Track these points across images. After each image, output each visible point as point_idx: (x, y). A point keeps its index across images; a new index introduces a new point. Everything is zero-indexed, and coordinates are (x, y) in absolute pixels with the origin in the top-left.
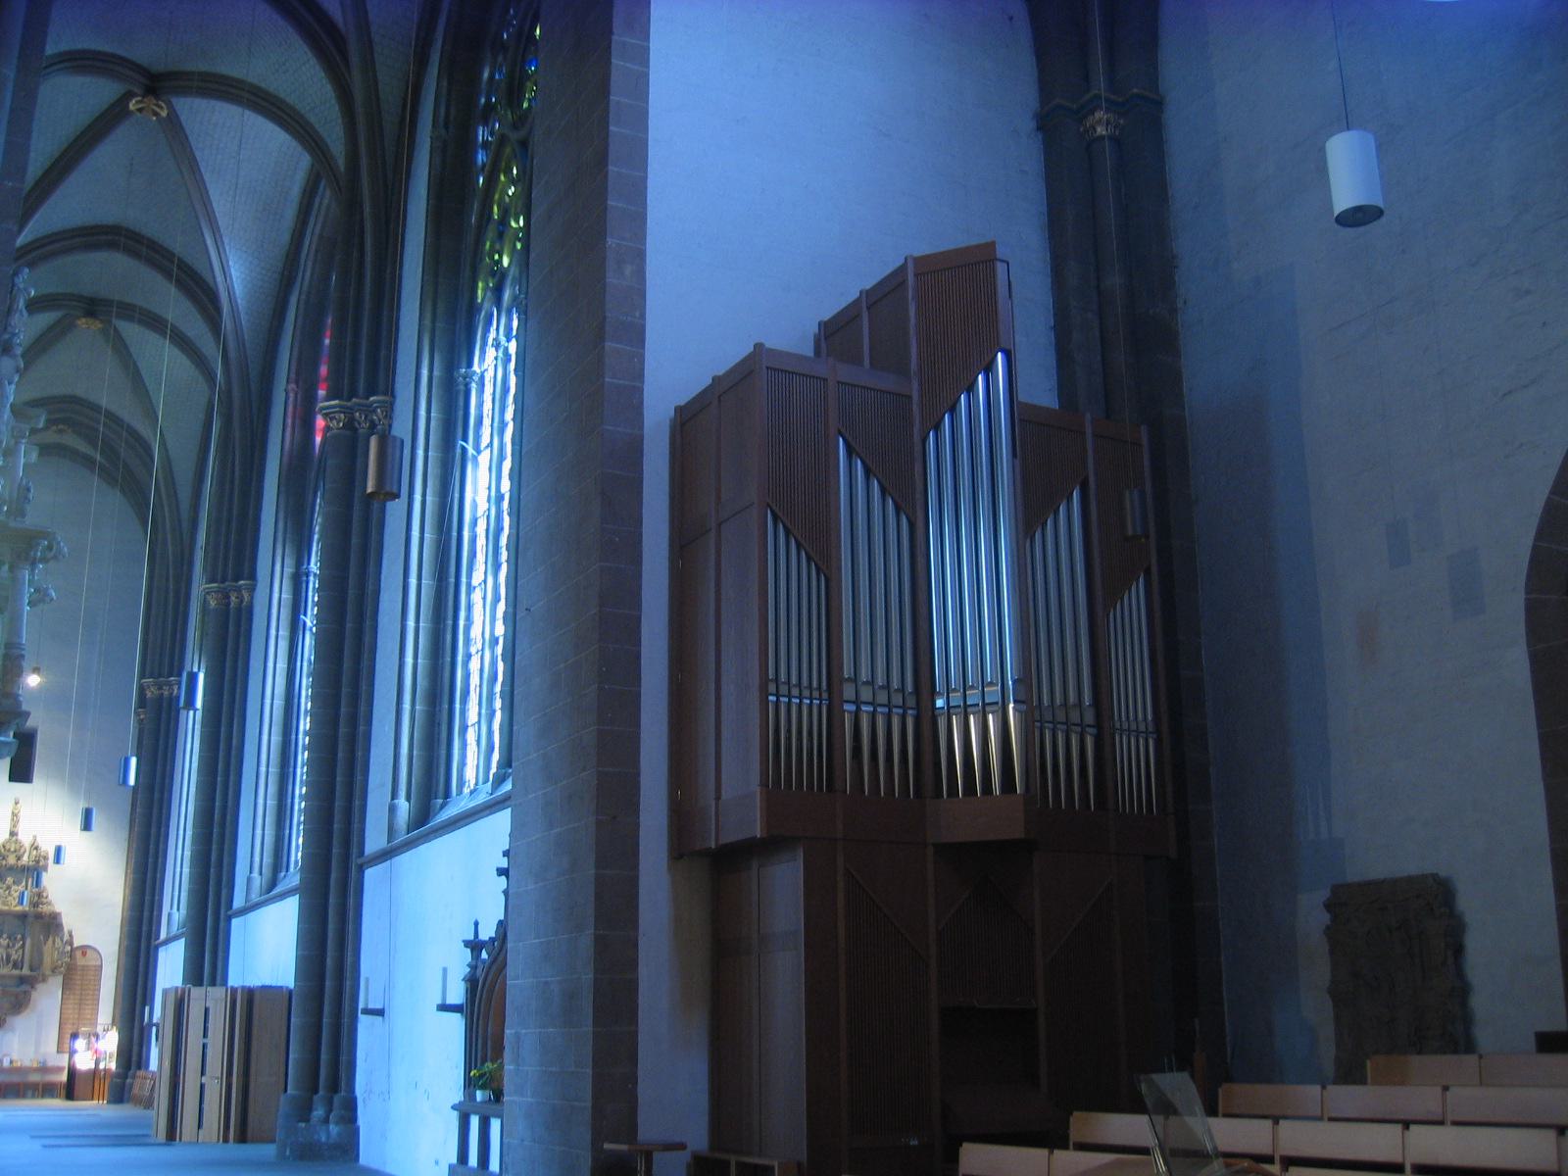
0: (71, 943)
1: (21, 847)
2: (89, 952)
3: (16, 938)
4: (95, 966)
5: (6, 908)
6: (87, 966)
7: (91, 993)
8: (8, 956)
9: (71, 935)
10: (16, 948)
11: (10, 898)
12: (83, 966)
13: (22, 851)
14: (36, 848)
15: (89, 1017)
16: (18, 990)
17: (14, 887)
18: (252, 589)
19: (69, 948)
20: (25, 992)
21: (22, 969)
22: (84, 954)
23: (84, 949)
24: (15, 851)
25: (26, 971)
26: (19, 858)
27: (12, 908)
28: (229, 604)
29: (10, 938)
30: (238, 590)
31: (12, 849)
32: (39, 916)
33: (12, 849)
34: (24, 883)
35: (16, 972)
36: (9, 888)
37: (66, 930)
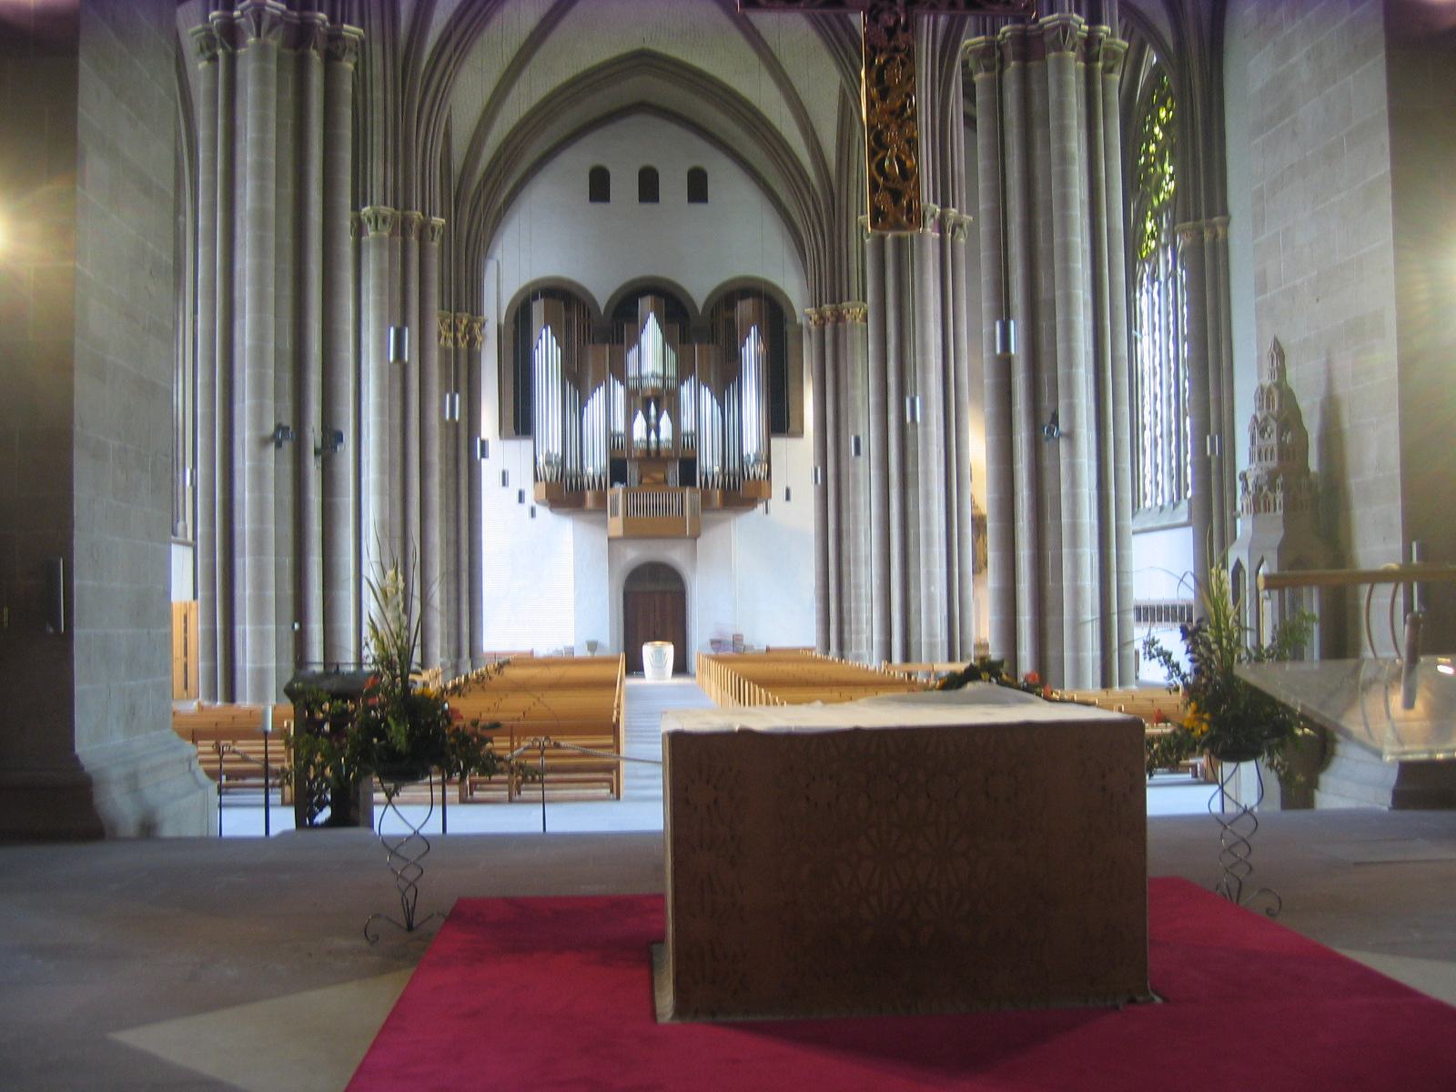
18: (1226, 224)
28: (1202, 240)
30: (1213, 227)
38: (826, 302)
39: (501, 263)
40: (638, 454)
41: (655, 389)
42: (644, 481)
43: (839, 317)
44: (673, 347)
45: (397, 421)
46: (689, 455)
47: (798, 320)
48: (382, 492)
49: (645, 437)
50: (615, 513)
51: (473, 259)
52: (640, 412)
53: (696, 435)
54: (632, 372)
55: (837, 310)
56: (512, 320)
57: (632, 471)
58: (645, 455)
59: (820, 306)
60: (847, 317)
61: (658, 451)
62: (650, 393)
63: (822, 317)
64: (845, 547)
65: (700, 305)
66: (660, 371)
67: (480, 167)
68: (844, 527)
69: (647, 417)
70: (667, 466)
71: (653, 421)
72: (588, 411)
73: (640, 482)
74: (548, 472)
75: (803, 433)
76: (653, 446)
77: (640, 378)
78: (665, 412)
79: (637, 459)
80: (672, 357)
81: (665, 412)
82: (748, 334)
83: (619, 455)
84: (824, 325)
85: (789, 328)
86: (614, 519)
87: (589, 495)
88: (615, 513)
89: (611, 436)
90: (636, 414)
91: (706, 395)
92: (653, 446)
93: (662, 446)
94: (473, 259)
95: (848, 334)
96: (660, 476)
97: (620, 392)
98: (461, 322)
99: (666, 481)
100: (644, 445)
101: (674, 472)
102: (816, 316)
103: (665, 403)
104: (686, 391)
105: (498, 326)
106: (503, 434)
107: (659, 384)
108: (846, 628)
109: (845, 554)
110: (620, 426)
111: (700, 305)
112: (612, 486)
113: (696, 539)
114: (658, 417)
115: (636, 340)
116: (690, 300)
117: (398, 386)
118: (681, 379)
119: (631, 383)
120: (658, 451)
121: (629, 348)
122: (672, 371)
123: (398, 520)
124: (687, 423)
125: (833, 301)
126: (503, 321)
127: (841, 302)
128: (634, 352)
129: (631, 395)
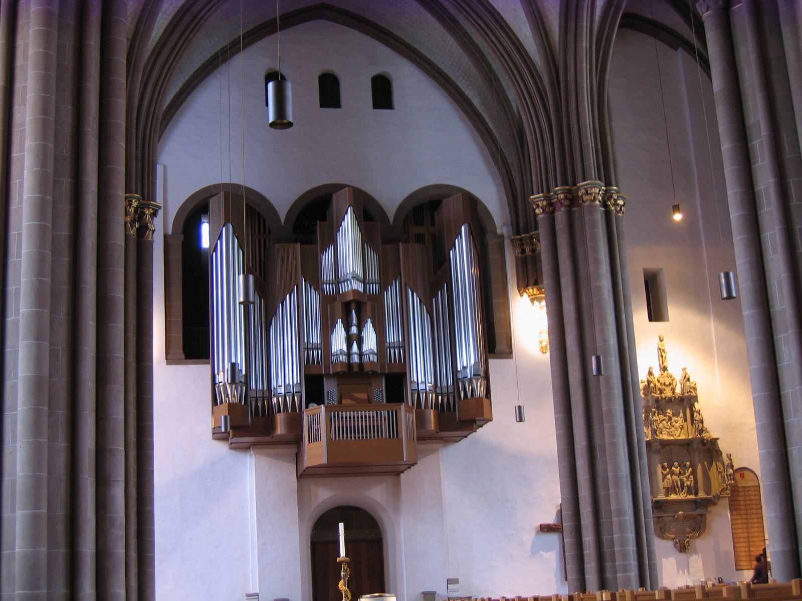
0: (732, 467)
1: (673, 380)
2: (746, 473)
3: (685, 466)
4: (754, 486)
5: (672, 438)
6: (747, 487)
7: (754, 511)
8: (682, 482)
9: (729, 456)
10: (687, 474)
11: (673, 429)
12: (744, 487)
13: (674, 384)
14: (688, 380)
15: (756, 534)
16: (696, 513)
17: (674, 418)
19: (731, 471)
20: (701, 515)
21: (696, 494)
22: (742, 476)
23: (742, 470)
24: (670, 384)
25: (701, 495)
26: (673, 390)
27: (677, 438)
29: (679, 465)
31: (667, 383)
32: (703, 442)
33: (667, 383)
34: (681, 414)
35: (692, 497)
36: (670, 419)
37: (724, 456)
38: (556, 186)
39: (170, 171)
40: (339, 369)
41: (355, 292)
42: (345, 401)
43: (573, 200)
44: (375, 249)
45: (65, 232)
46: (398, 370)
47: (499, 231)
48: (38, 334)
49: (345, 348)
50: (314, 438)
51: (145, 134)
52: (339, 321)
53: (405, 345)
54: (327, 273)
55: (569, 191)
56: (181, 229)
57: (330, 388)
58: (345, 369)
59: (548, 191)
60: (585, 198)
61: (361, 365)
62: (351, 298)
63: (550, 204)
64: (599, 466)
65: (391, 215)
66: (360, 273)
67: (153, 35)
68: (597, 441)
69: (347, 328)
70: (370, 384)
71: (354, 330)
72: (277, 322)
73: (340, 402)
74: (232, 394)
75: (512, 353)
76: (356, 359)
77: (337, 281)
78: (369, 321)
79: (336, 375)
80: (373, 258)
81: (369, 321)
82: (460, 234)
83: (314, 372)
84: (553, 212)
85: (491, 240)
86: (313, 445)
87: (280, 418)
88: (314, 438)
89: (304, 348)
90: (333, 326)
91: (414, 300)
92: (356, 359)
93: (365, 359)
94: (145, 134)
95: (587, 218)
96: (363, 396)
97: (315, 299)
98: (130, 205)
99: (369, 401)
100: (344, 359)
101: (380, 390)
102: (545, 203)
103: (369, 307)
104: (391, 299)
105: (165, 236)
106: (170, 358)
107: (360, 287)
108: (608, 565)
109: (600, 475)
110: (316, 339)
111: (391, 215)
112: (307, 407)
113: (398, 473)
114: (360, 328)
115: (331, 239)
116: (379, 207)
117: (66, 182)
118: (384, 285)
119: (326, 288)
120: (361, 365)
121: (324, 249)
122: (374, 274)
123: (62, 380)
124: (392, 336)
125: (565, 183)
126: (170, 232)
127: (575, 184)
128: (330, 251)
129: (327, 301)
